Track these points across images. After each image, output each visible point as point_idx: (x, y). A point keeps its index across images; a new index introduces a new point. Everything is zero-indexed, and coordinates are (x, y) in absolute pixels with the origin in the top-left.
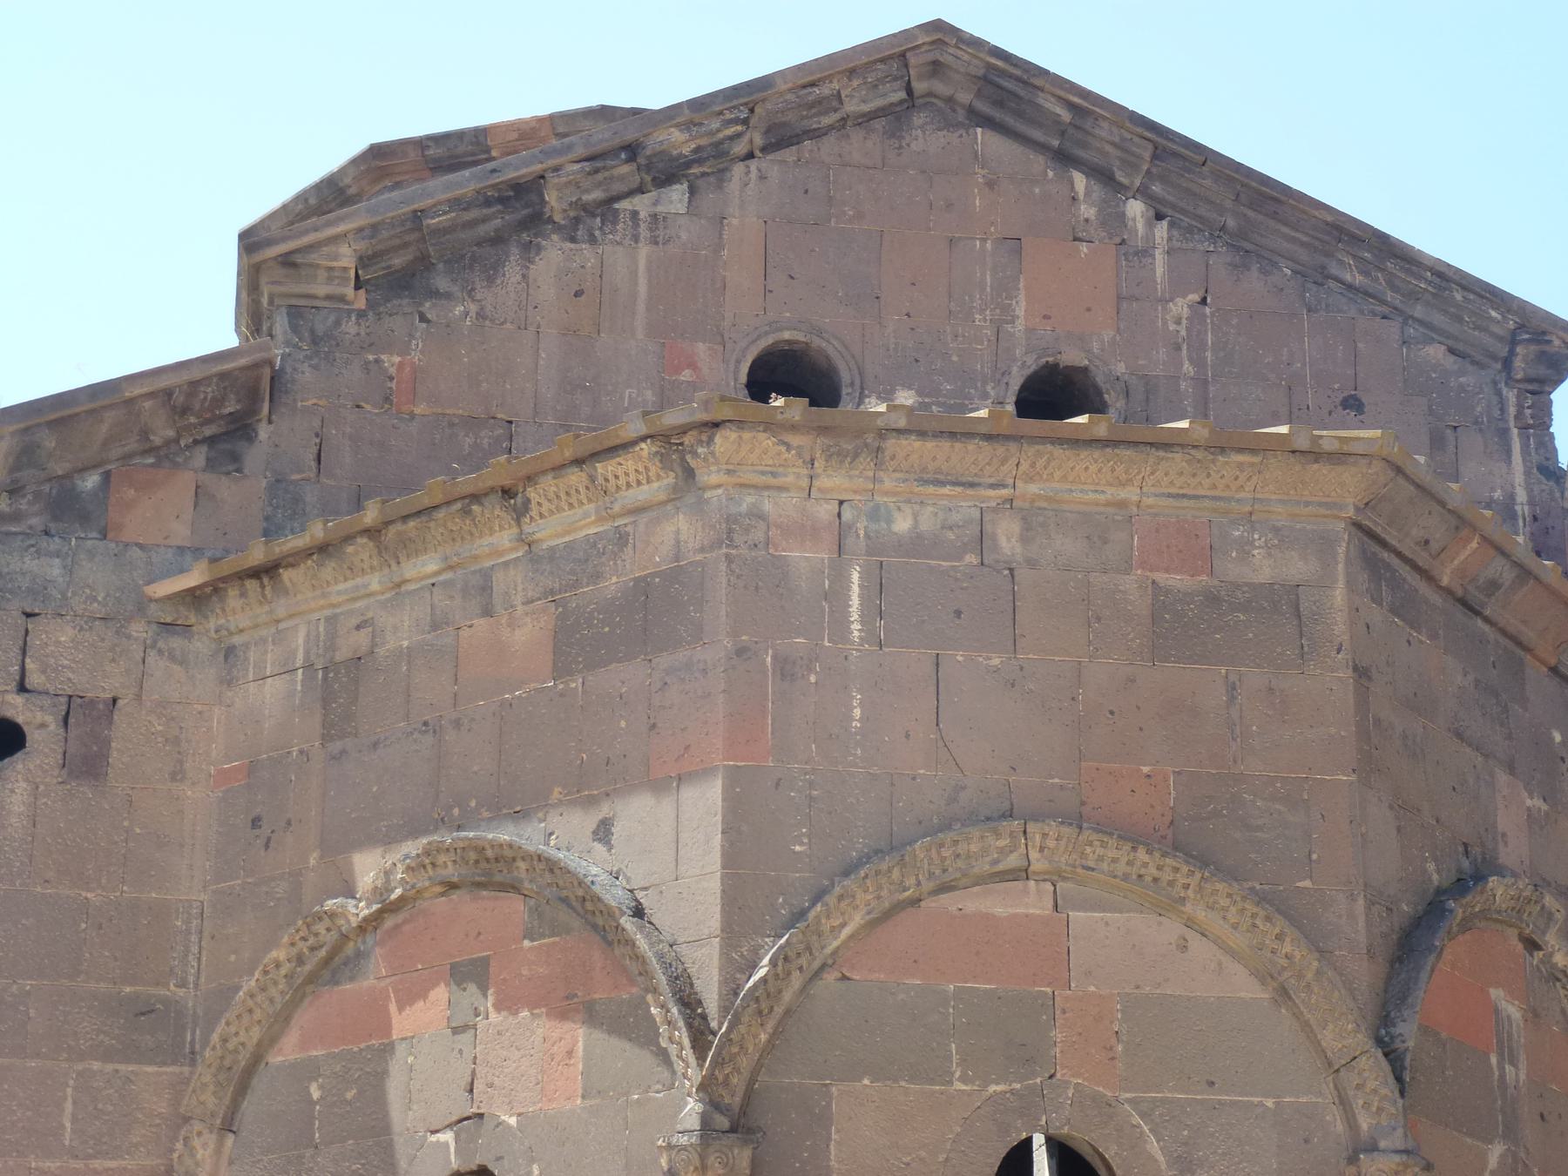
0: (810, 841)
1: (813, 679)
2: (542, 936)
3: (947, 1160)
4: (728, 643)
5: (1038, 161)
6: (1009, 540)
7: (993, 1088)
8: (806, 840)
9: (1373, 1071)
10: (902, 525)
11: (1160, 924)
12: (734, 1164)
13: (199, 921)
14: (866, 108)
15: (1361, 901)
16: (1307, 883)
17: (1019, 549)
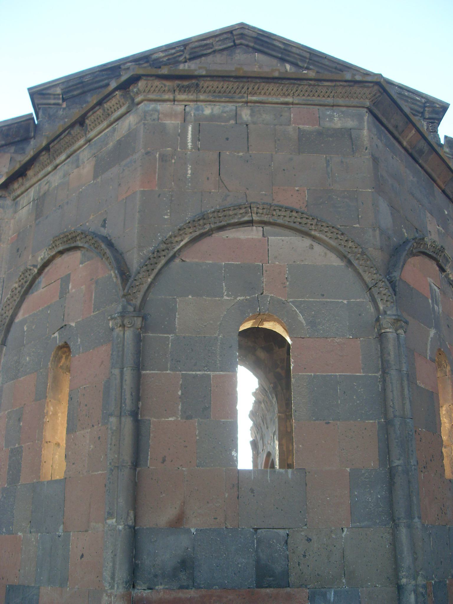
0: (171, 214)
1: (173, 161)
2: (85, 262)
3: (221, 324)
4: (143, 151)
5: (275, 62)
6: (246, 115)
7: (238, 298)
8: (169, 214)
9: (384, 289)
10: (207, 111)
11: (303, 240)
12: (134, 323)
13: (3, 283)
14: (221, 48)
15: (378, 231)
16: (358, 225)
17: (249, 118)
